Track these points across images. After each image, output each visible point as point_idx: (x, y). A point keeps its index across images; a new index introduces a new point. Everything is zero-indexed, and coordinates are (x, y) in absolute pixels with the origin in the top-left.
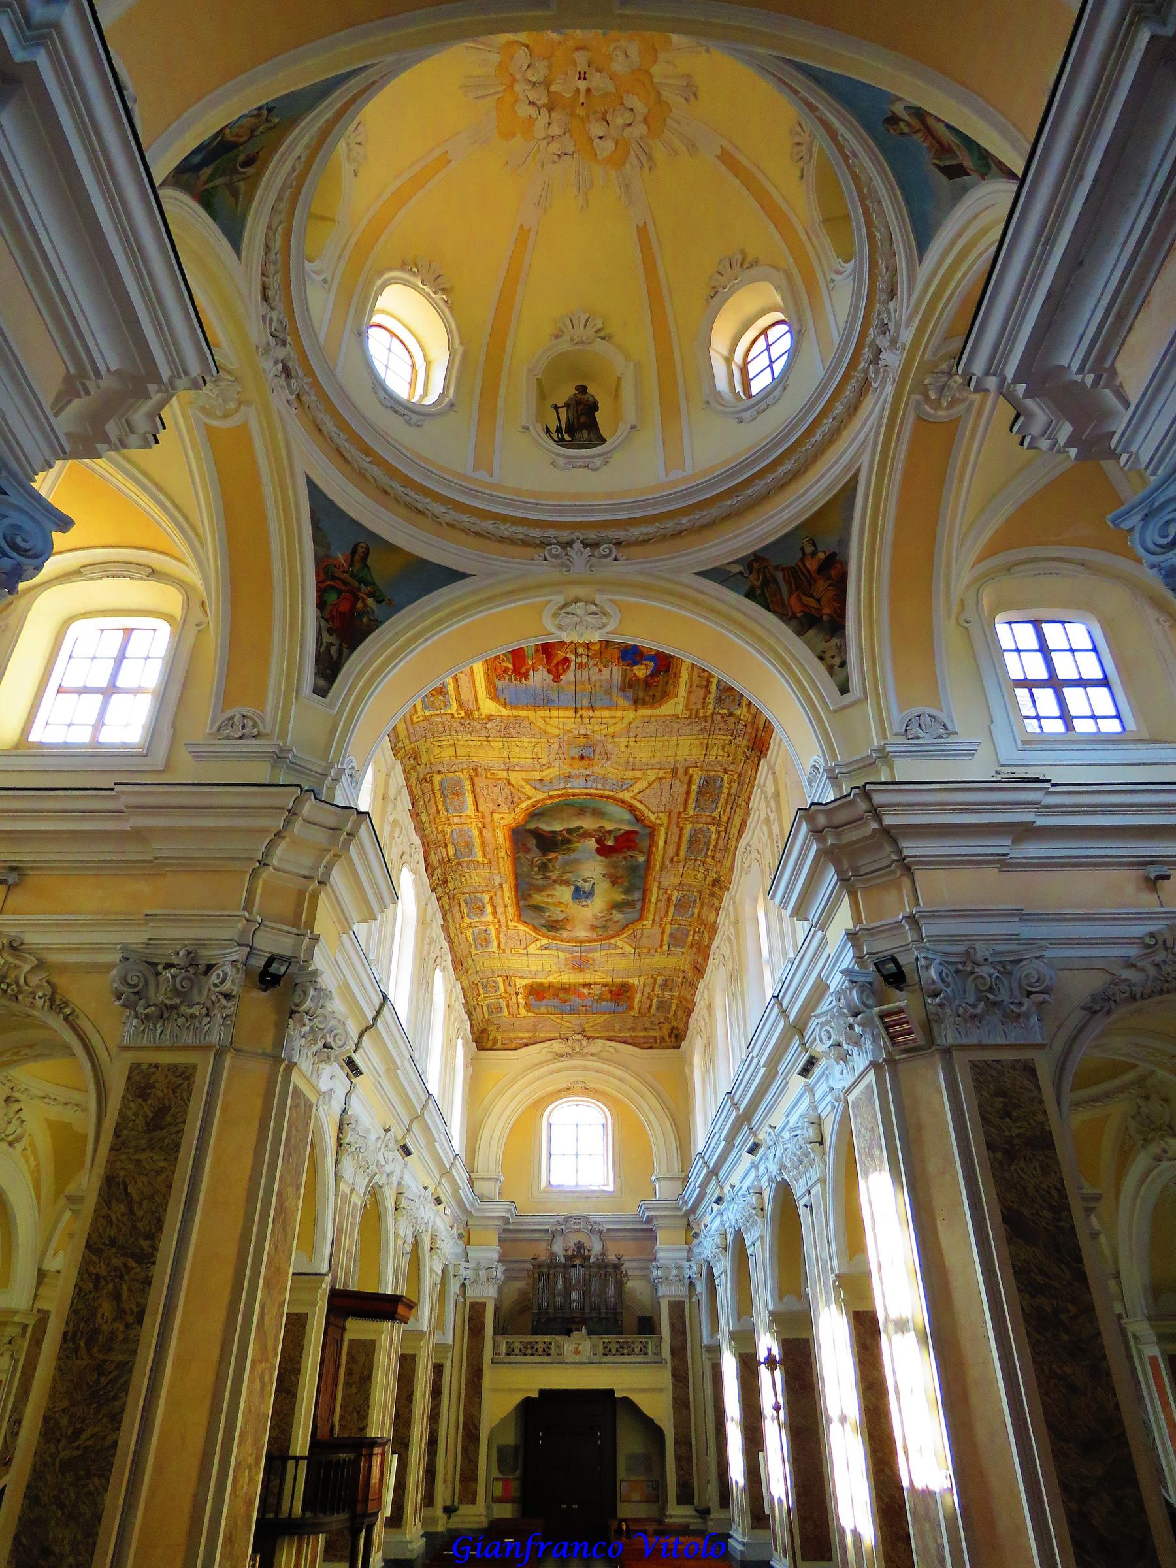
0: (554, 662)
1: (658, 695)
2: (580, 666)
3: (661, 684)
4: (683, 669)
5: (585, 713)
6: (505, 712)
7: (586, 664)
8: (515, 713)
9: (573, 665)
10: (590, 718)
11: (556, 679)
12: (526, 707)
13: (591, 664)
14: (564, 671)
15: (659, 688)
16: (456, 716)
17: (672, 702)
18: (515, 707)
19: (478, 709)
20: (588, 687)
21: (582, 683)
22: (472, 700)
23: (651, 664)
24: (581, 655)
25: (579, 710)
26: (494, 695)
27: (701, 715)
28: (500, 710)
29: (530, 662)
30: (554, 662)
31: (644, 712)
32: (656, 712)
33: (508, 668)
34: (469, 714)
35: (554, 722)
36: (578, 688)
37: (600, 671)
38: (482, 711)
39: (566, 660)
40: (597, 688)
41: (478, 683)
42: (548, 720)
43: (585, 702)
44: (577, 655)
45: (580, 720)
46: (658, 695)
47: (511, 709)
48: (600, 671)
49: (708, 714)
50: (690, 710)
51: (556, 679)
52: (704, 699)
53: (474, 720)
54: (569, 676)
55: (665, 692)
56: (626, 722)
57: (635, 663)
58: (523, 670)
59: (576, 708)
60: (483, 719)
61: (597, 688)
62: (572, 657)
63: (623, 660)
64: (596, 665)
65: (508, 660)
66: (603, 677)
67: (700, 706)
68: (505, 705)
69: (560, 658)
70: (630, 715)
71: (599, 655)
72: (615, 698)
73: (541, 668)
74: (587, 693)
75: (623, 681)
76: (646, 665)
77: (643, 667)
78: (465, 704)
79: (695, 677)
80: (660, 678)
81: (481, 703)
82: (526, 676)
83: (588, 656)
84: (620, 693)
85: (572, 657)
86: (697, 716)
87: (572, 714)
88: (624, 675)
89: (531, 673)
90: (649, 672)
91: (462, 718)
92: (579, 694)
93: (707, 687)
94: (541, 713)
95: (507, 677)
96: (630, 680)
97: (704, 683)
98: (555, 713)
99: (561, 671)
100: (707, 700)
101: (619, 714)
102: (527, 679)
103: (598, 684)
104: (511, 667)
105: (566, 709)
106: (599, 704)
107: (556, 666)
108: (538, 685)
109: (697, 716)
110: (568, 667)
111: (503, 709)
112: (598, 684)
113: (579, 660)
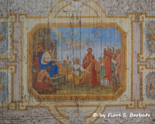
0: (90, 65)
1: (38, 37)
2: (77, 61)
3: (37, 46)
4: (26, 57)
5: (76, 21)
6: (117, 21)
7: (74, 64)
8: (112, 20)
9: (81, 63)
10: (73, 17)
11: (90, 50)
12: (107, 25)
13: (72, 64)
14: (86, 57)
15: (37, 43)
16: (144, 16)
17: (30, 30)
18: (112, 25)
19: (132, 21)
20: (74, 45)
21: (77, 49)
22: (134, 32)
23: (42, 63)
24: (77, 70)
25: (78, 24)
26: (123, 34)
27: (13, 17)
28: (121, 22)
29: (102, 64)
30: (90, 65)
31: (44, 21)
32: (38, 22)
33: (114, 59)
34: (137, 18)
35: (92, 13)
36: (78, 45)
37: (68, 58)
38: (130, 21)
39: (85, 67)
40: (69, 43)
41: (130, 44)
42: (95, 15)
43: (75, 31)
44: (79, 70)
45: (79, 15)
46: (38, 37)
47: (114, 24)
48: (68, 58)
49: (10, 17)
50: (20, 22)
51: (90, 50)
52: (13, 31)
53: (135, 13)
54: (84, 52)
55: (34, 39)
56: (53, 14)
57: (50, 63)
58: (107, 57)
59: (80, 26)
60: (130, 13)
61: (69, 43)
62: (82, 69)
63: (56, 66)
64: (70, 62)
65: (113, 63)
66: (66, 52)
67: (15, 24)
68: (118, 28)
69: (88, 68)
70: (52, 20)
71: (69, 70)
72: (60, 34)
73: (98, 60)
74: (74, 40)
75: (56, 49)
76: (45, 62)
77: (46, 60)
78: (138, 27)
79: (19, 50)
80: (37, 51)
81: (130, 29)
82: (106, 53)
83: (74, 70)
84: (57, 39)
85: (82, 69)
86: (16, 15)
87: (83, 21)
88: (56, 53)
89: (103, 56)
90: (43, 56)
91: (141, 14)
92: (78, 38)
93: (13, 41)
94: (99, 21)
95: (115, 52)
96: (52, 50)
97: (15, 44)
98: (91, 21)
99: (88, 57)
100: (11, 29)
101: (58, 21)
102: (105, 51)
103: (69, 47)
104: (113, 60)
105: (86, 25)
106: (68, 29)
107: (89, 63)
108: (99, 46)
109: (16, 15)
110: (84, 61)
111: (119, 24)
112: (69, 47)
113: (79, 66)
